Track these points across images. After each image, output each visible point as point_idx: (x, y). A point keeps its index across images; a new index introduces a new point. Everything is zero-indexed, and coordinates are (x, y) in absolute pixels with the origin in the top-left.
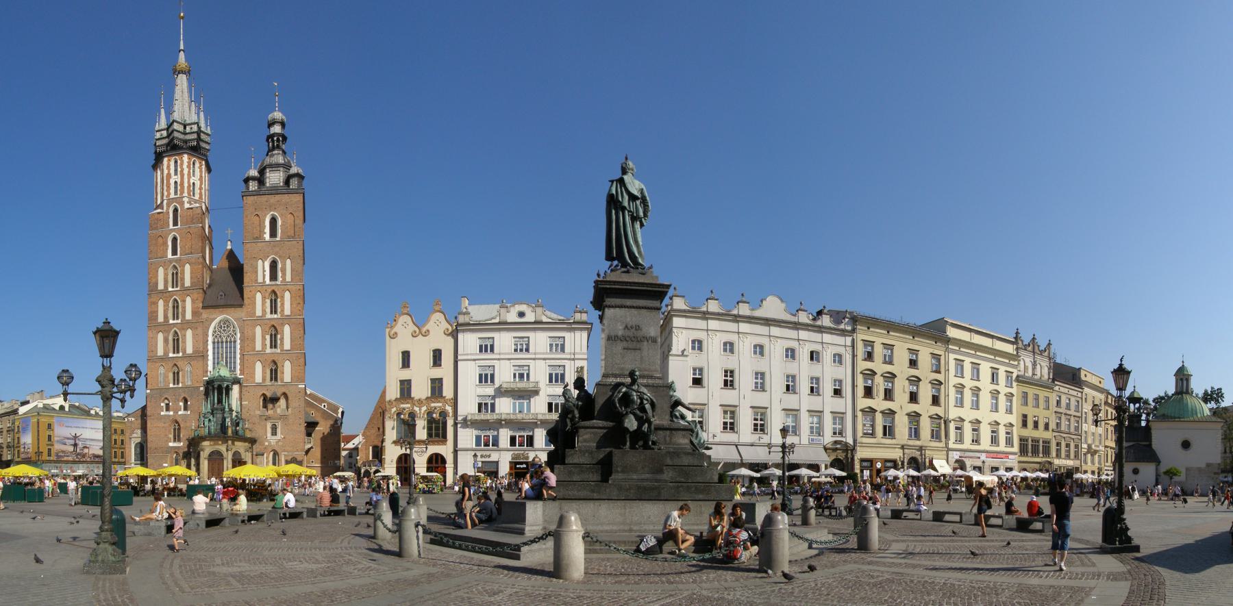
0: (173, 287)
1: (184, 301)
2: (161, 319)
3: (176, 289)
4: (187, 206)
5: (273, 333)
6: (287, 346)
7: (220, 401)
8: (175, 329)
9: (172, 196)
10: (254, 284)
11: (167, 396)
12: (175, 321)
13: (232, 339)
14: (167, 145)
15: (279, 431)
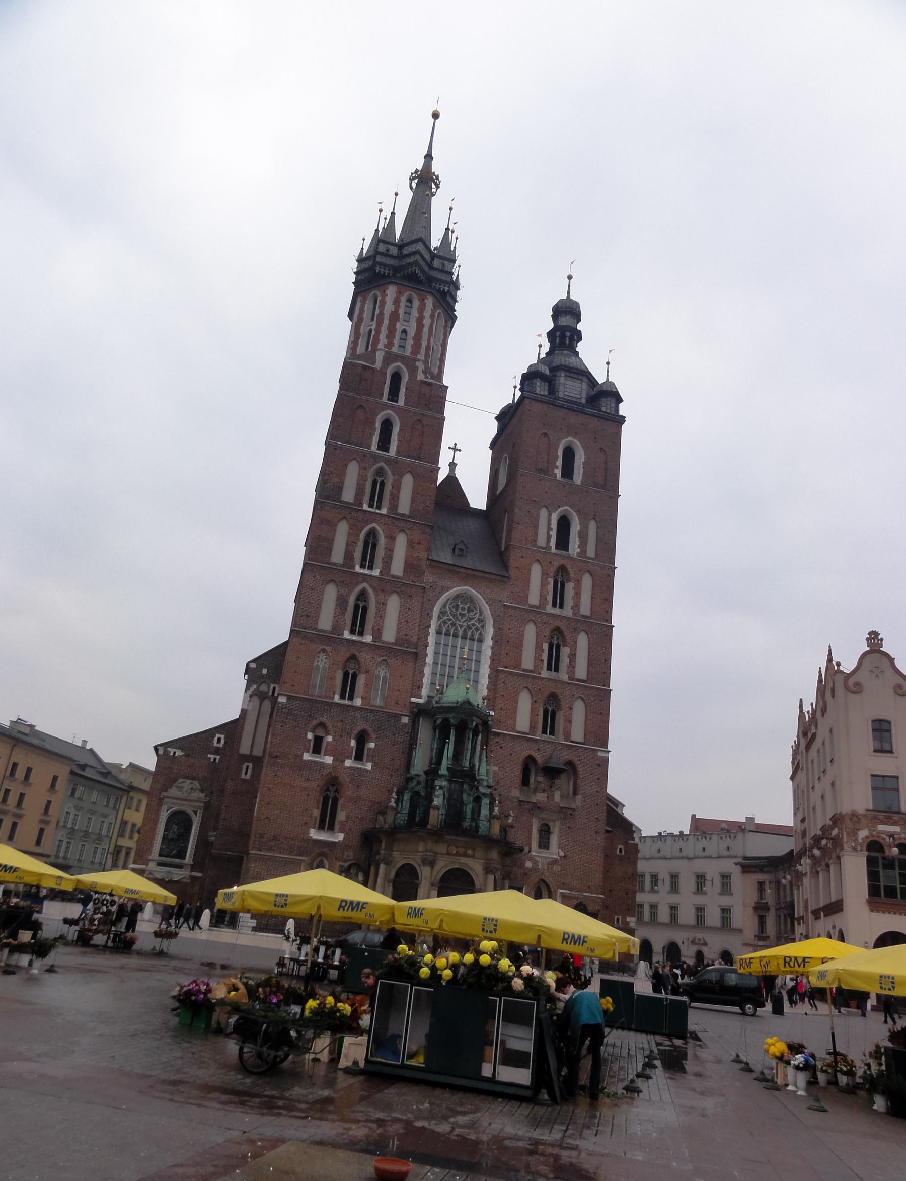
0: (371, 506)
1: (391, 538)
2: (337, 556)
3: (377, 511)
4: (420, 376)
5: (555, 643)
6: (581, 671)
7: (458, 755)
8: (365, 585)
9: (395, 349)
10: (529, 546)
11: (324, 720)
12: (366, 571)
13: (476, 636)
14: (396, 270)
15: (554, 839)
